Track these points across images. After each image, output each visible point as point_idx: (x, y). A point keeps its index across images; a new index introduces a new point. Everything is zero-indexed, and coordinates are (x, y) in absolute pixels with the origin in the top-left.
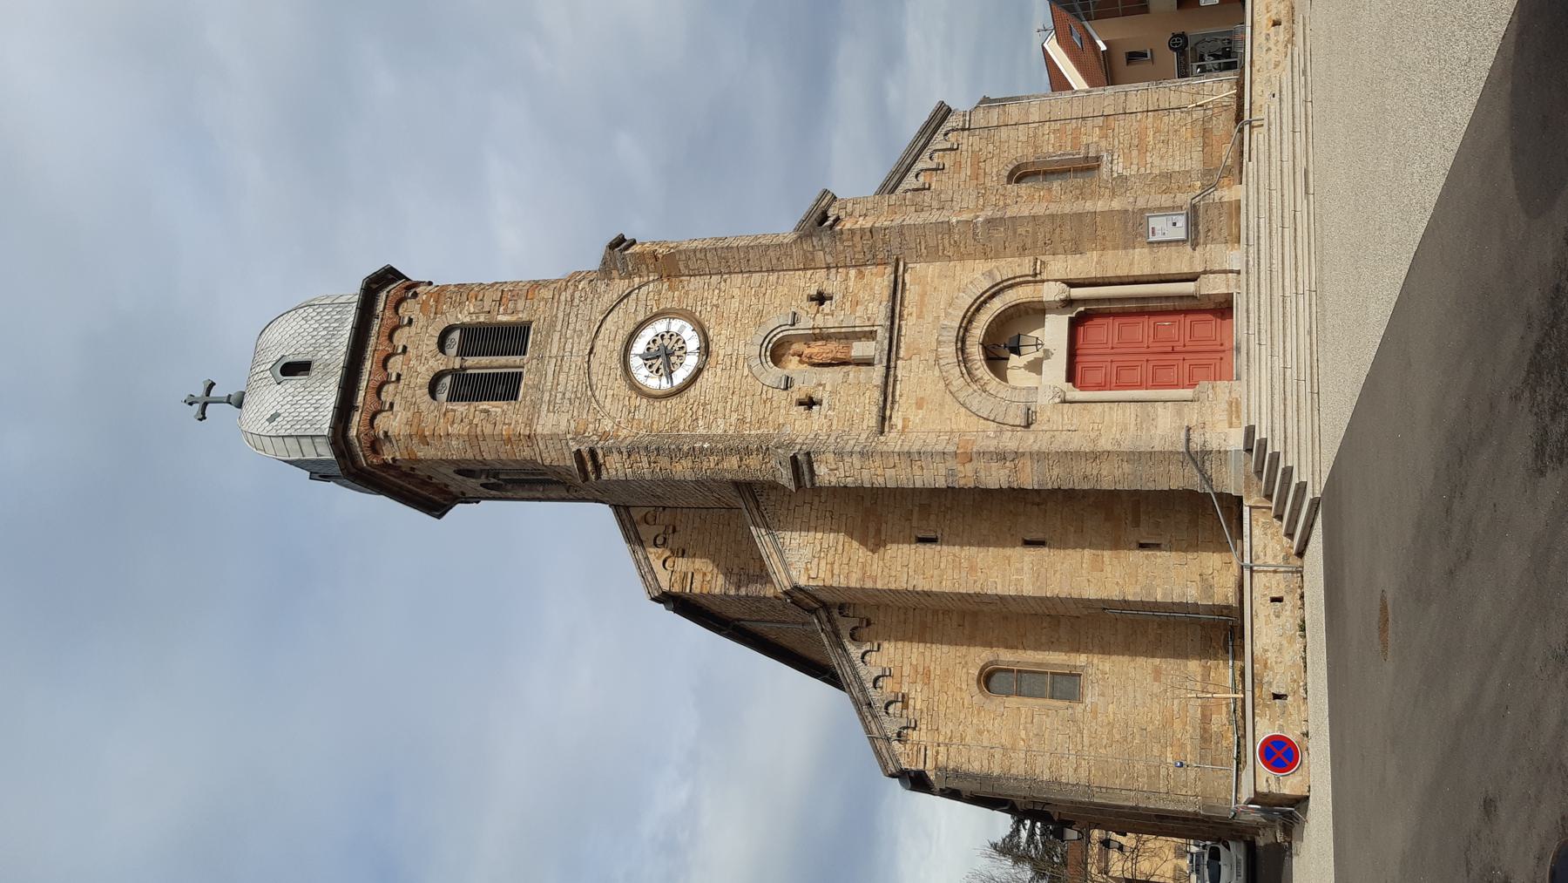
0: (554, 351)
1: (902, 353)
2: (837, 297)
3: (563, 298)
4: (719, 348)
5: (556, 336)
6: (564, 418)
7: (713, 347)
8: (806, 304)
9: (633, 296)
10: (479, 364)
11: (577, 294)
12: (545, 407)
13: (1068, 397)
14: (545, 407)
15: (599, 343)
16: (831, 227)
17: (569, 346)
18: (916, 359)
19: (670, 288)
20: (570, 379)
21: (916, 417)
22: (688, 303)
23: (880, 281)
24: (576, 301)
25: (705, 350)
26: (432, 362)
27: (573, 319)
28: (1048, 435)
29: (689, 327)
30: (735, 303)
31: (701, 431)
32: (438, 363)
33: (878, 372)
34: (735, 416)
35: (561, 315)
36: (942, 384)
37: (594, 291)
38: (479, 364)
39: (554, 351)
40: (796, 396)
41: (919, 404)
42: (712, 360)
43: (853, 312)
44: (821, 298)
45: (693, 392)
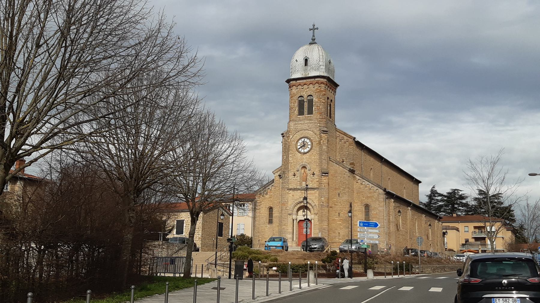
0: (305, 122)
1: (302, 191)
2: (313, 178)
3: (316, 121)
4: (305, 156)
5: (308, 122)
6: (292, 128)
7: (305, 155)
8: (312, 172)
9: (316, 136)
10: (306, 105)
11: (316, 124)
12: (295, 123)
13: (295, 221)
14: (295, 123)
15: (307, 131)
16: (322, 175)
17: (306, 125)
18: (300, 194)
19: (317, 143)
20: (299, 127)
21: (291, 195)
22: (314, 148)
23: (315, 186)
24: (315, 124)
25: (305, 153)
26: (306, 95)
27: (312, 124)
28: (287, 218)
29: (309, 149)
30: (313, 158)
31: (290, 155)
32: (305, 96)
33: (298, 187)
34: (292, 161)
35: (312, 121)
36: (296, 199)
37: (317, 128)
38: (306, 105)
39: (305, 122)
40: (295, 173)
41: (293, 195)
42: (303, 155)
43: (310, 181)
44: (314, 174)
45: (297, 152)
